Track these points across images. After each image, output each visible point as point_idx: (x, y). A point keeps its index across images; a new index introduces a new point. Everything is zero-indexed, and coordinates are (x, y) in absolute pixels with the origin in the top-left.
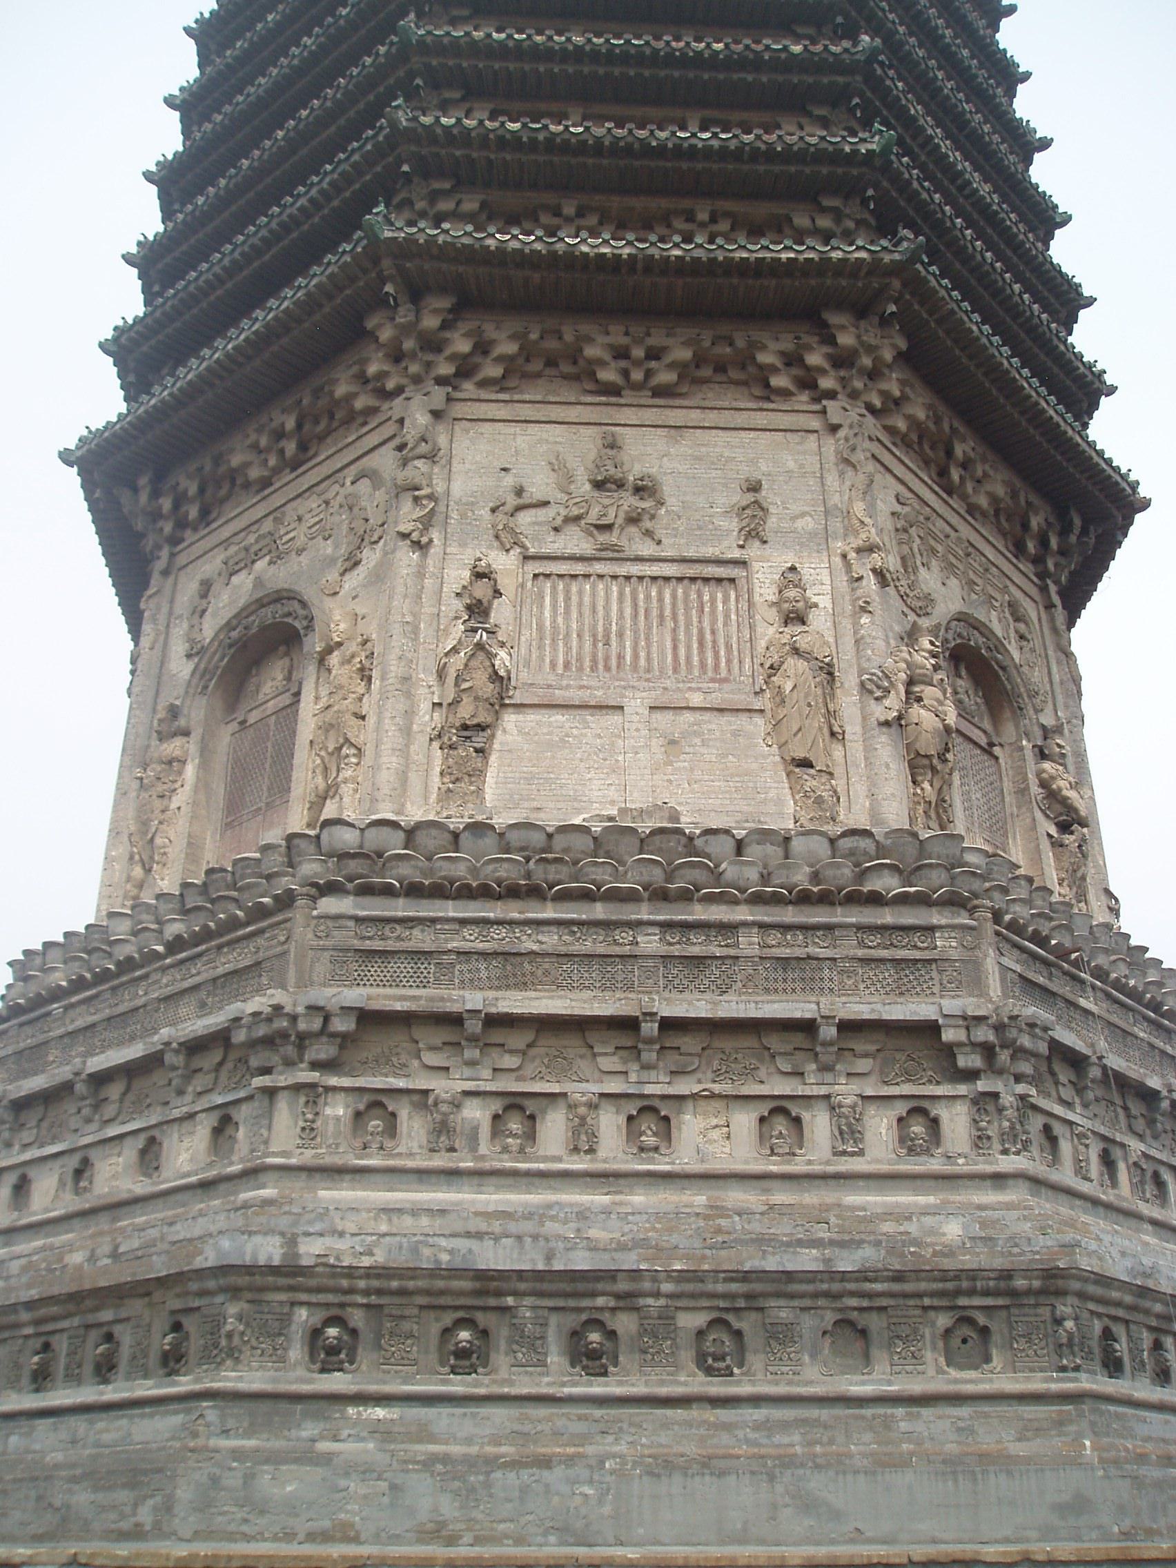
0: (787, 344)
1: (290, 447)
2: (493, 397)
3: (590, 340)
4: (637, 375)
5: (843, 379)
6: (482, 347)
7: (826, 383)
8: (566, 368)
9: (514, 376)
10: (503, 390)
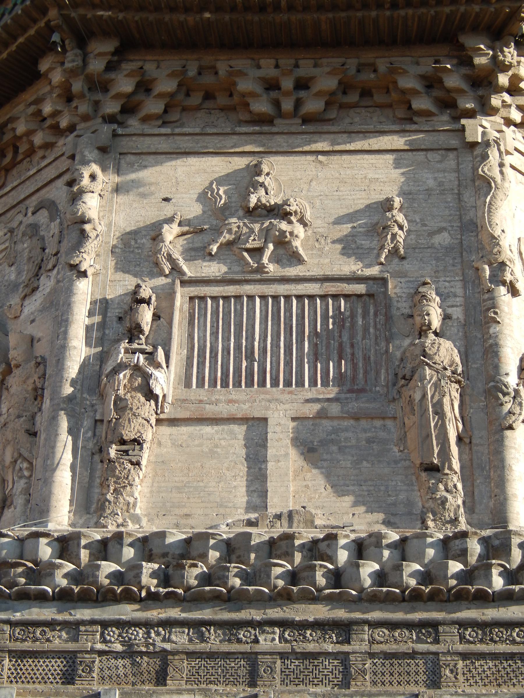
2: (156, 131)
3: (241, 74)
4: (287, 105)
6: (144, 86)
8: (222, 100)
9: (174, 110)
10: (165, 124)
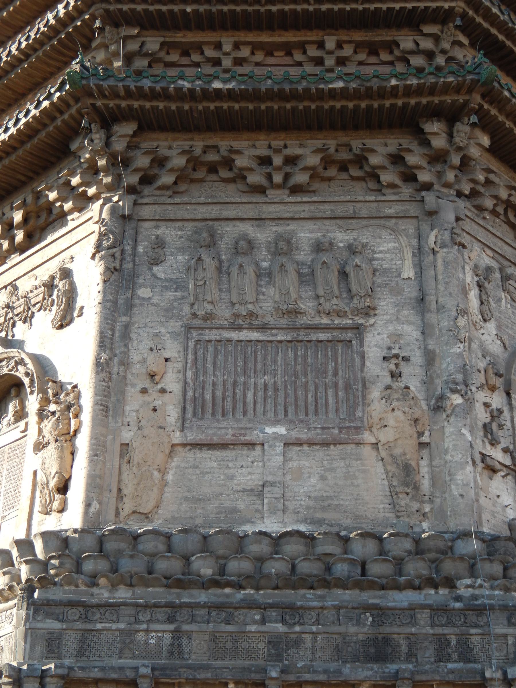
0: (392, 149)
4: (278, 178)
5: (439, 172)
7: (424, 177)
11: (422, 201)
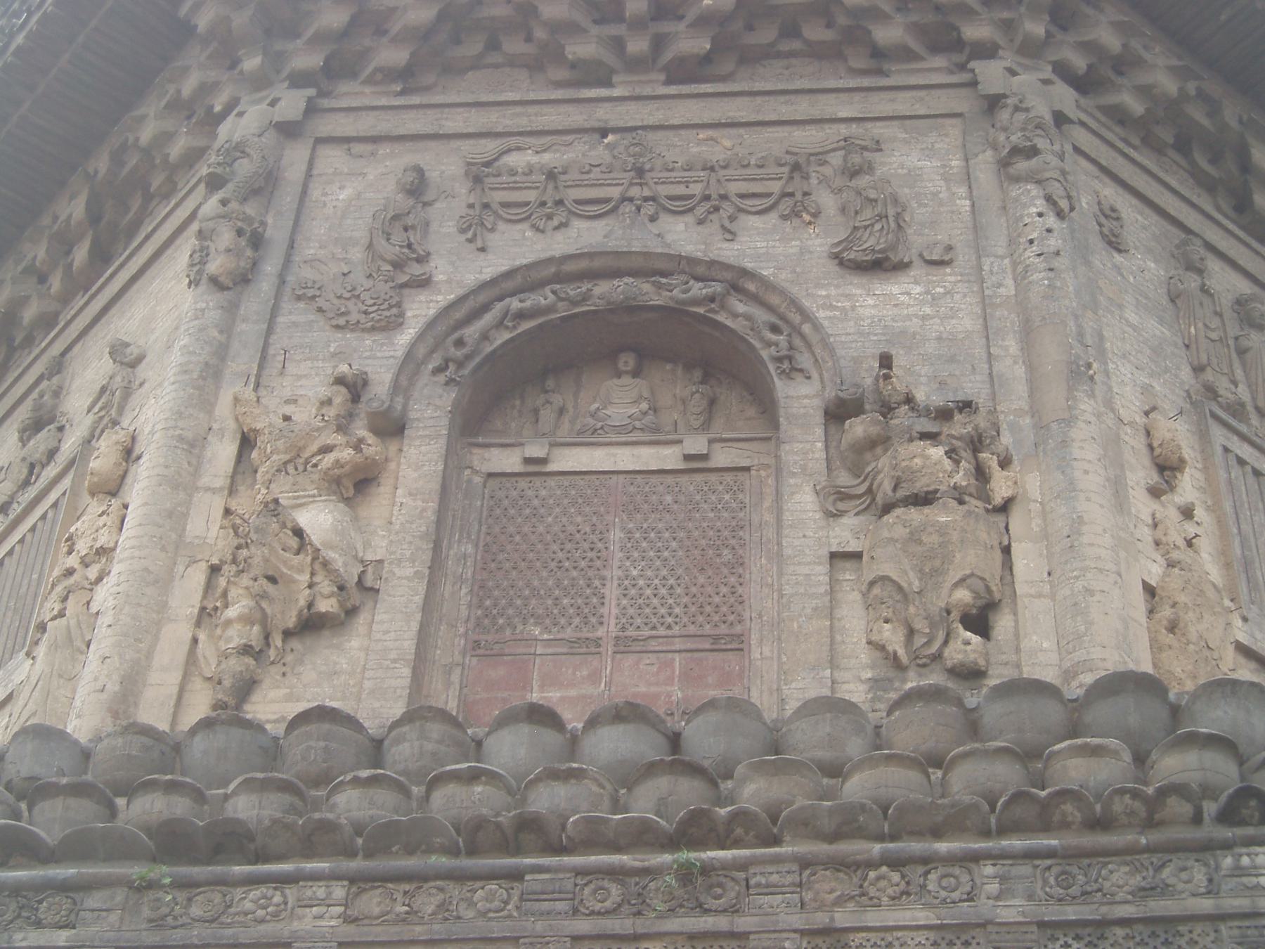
1: (81, 254)
11: (974, 84)
